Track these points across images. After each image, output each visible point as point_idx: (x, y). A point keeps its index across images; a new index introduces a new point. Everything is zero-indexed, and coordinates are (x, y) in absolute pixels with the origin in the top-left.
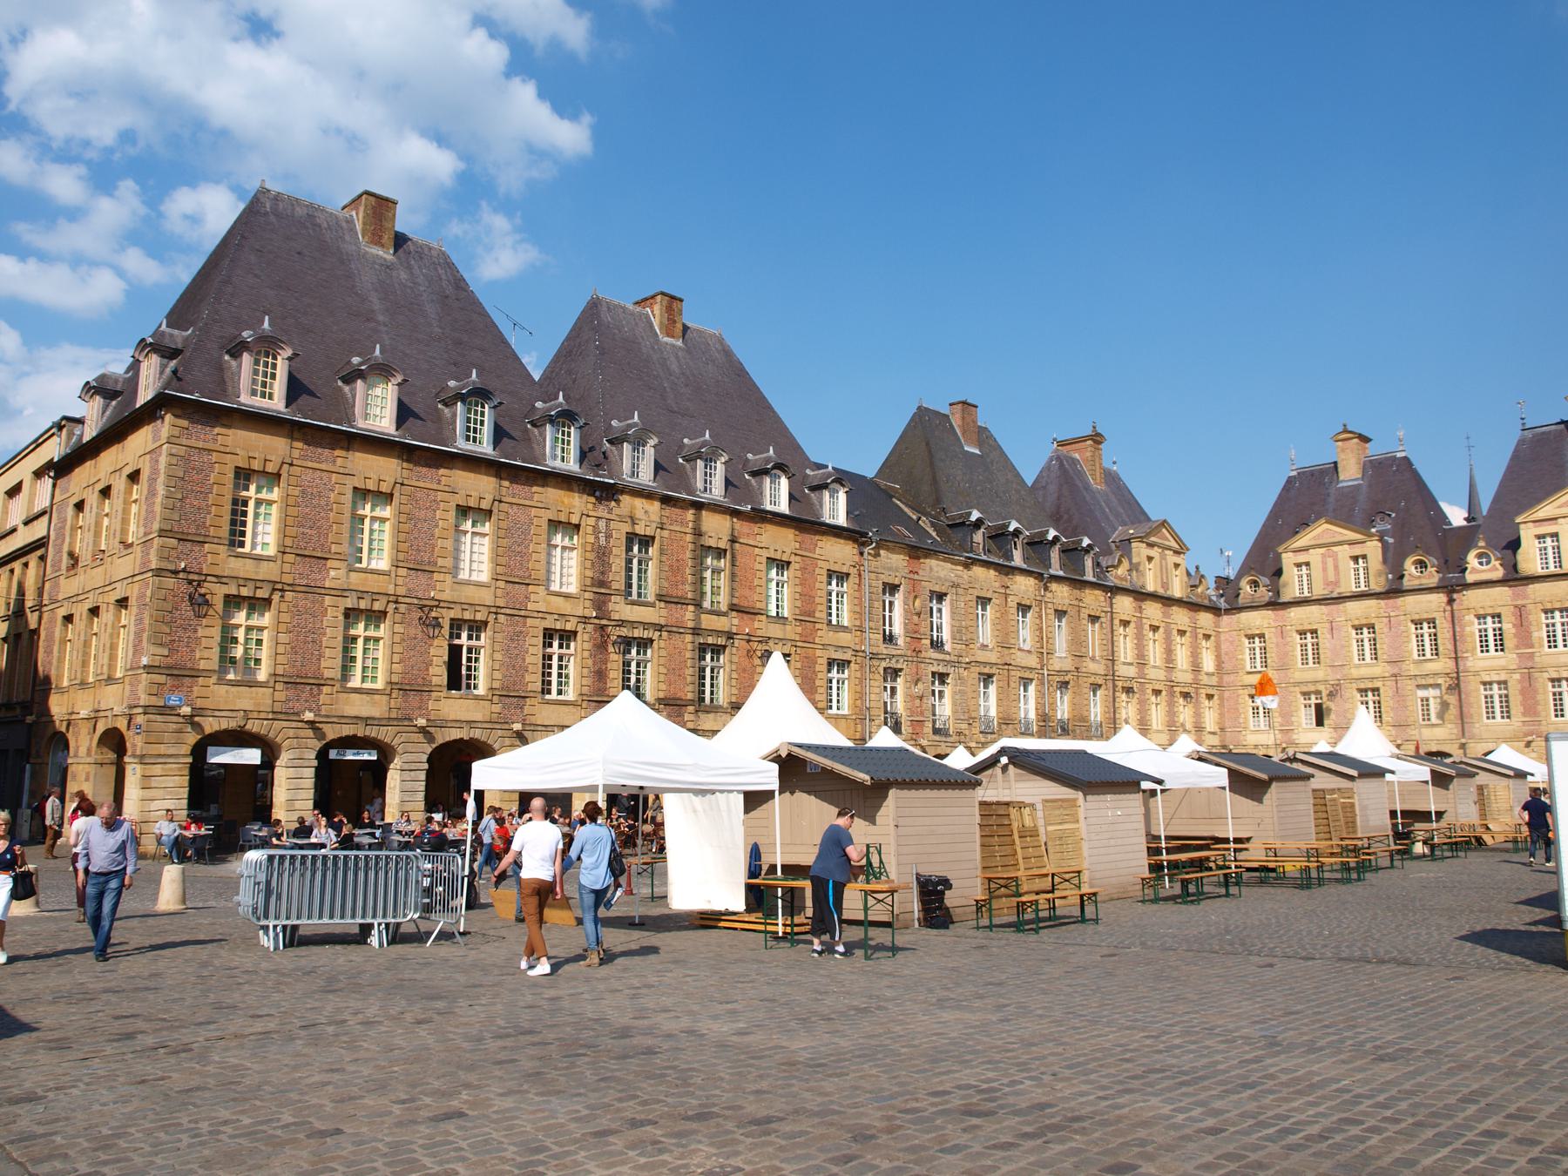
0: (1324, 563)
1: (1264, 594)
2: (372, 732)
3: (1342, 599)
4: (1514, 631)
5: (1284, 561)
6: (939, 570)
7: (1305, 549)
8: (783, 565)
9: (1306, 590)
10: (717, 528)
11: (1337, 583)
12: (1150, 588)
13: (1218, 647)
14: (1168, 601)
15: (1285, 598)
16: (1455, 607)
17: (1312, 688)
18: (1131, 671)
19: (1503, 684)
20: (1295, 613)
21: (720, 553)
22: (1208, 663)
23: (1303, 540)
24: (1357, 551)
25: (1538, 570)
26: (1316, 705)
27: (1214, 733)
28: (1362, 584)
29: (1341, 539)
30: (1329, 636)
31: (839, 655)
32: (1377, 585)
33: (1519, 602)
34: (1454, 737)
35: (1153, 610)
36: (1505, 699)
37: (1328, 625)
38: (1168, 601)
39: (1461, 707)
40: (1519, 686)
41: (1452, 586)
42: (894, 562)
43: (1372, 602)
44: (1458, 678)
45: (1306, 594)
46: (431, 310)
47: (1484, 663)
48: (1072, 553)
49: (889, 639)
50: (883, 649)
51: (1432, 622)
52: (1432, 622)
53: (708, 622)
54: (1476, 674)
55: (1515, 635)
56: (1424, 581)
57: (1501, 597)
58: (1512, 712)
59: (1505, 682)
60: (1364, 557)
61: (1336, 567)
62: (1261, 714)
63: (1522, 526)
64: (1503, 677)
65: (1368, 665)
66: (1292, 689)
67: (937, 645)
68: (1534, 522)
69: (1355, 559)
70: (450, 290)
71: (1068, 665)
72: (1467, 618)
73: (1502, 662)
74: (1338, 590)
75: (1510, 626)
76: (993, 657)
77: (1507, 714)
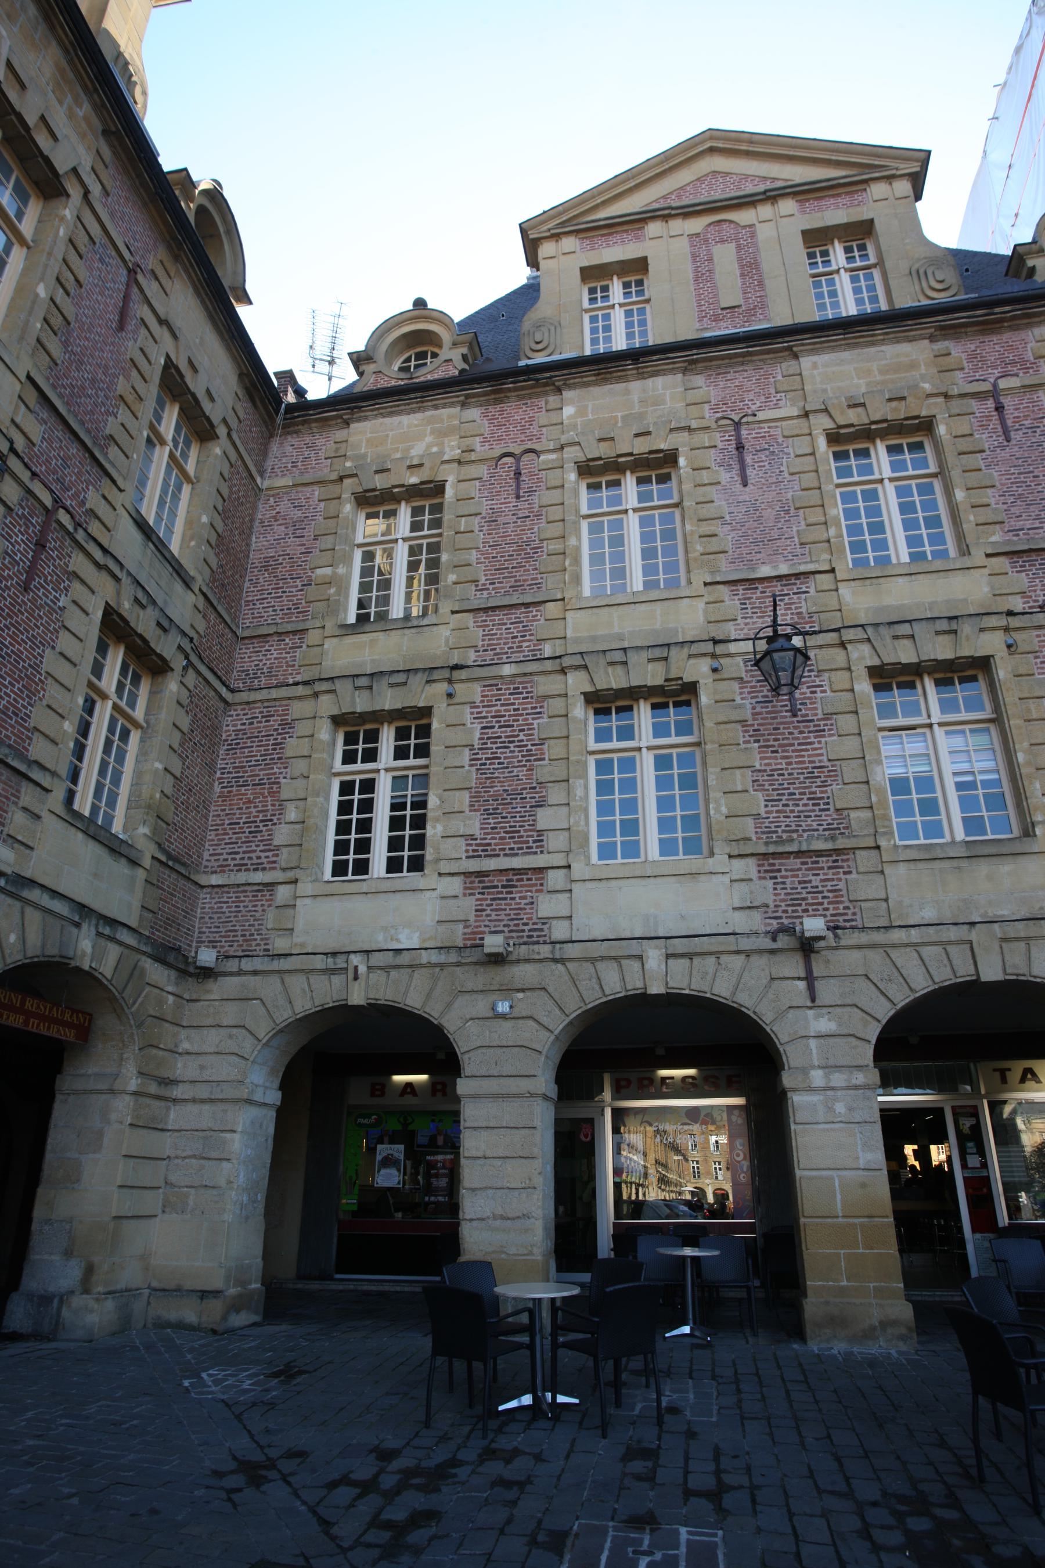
37: (722, 439)
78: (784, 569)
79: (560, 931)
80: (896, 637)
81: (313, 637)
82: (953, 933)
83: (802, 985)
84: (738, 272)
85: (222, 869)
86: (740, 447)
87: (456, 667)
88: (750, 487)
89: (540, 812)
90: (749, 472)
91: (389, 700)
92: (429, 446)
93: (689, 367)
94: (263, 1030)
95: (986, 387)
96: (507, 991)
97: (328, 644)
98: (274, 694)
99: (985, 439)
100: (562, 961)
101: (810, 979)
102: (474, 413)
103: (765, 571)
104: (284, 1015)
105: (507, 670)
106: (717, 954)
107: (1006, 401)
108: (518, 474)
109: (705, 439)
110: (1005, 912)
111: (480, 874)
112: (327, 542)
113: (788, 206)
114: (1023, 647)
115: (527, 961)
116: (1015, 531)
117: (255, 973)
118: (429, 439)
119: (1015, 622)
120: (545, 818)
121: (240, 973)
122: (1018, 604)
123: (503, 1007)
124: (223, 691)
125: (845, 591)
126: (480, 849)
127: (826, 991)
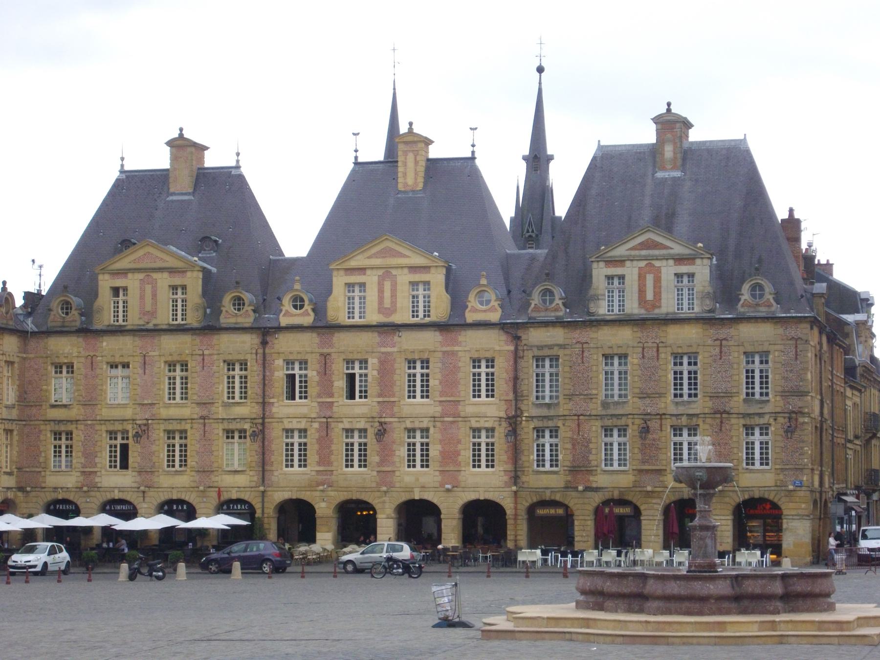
0: (142, 290)
1: (75, 319)
3: (157, 331)
4: (317, 379)
5: (100, 283)
7: (124, 273)
9: (121, 318)
11: (153, 314)
13: (21, 376)
15: (97, 326)
16: (267, 351)
17: (118, 427)
19: (303, 432)
20: (109, 346)
23: (125, 262)
24: (177, 281)
25: (344, 320)
26: (122, 445)
27: (10, 474)
28: (179, 317)
29: (159, 264)
30: (141, 371)
32: (193, 319)
33: (325, 351)
34: (254, 484)
36: (303, 447)
37: (140, 359)
39: (264, 454)
40: (317, 435)
43: (187, 338)
44: (263, 424)
45: (121, 322)
51: (244, 365)
52: (244, 365)
54: (280, 420)
55: (318, 384)
56: (240, 320)
58: (309, 461)
59: (305, 431)
60: (184, 287)
61: (154, 295)
62: (63, 454)
63: (335, 273)
64: (302, 426)
65: (177, 405)
66: (98, 427)
68: (347, 270)
69: (174, 288)
72: (277, 362)
73: (304, 410)
74: (154, 322)
75: (315, 373)
77: (303, 463)
78: (150, 402)
79: (99, 485)
80: (169, 423)
81: (44, 407)
82: (169, 490)
83: (142, 498)
84: (151, 297)
85: (29, 467)
86: (145, 363)
87: (78, 420)
88: (146, 376)
89: (96, 459)
90: (147, 371)
91: (63, 428)
92: (69, 350)
93: (134, 336)
94: (42, 503)
95: (201, 352)
96: (89, 497)
97: (48, 410)
98: (36, 423)
99: (198, 368)
100: (99, 491)
101: (144, 497)
102: (81, 340)
103: (146, 402)
104: (45, 500)
105: (89, 422)
106: (128, 492)
107: (206, 358)
108: (92, 363)
109: (137, 359)
110: (179, 486)
111: (84, 472)
112: (44, 378)
113: (166, 275)
114: (194, 427)
115: (93, 491)
116: (199, 396)
117: (39, 491)
118: (69, 347)
119: (193, 421)
120: (97, 460)
121: (35, 491)
122: (195, 416)
123: (88, 500)
124: (24, 423)
125: (162, 410)
126: (84, 466)
127: (147, 499)
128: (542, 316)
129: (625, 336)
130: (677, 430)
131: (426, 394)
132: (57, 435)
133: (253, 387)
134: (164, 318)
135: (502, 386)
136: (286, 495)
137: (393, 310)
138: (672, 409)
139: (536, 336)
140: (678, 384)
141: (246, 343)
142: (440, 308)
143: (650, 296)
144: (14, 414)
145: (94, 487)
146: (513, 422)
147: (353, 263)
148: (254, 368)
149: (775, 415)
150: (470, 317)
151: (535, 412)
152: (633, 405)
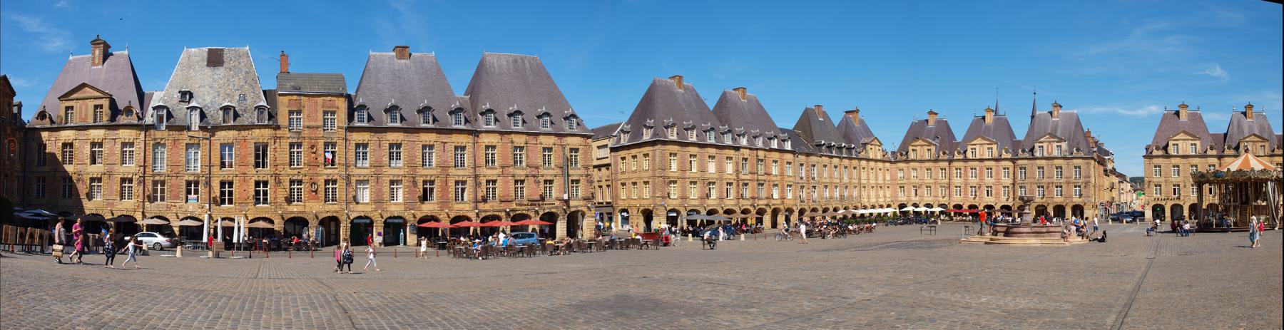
2: (696, 208)
6: (813, 159)
8: (776, 162)
10: (761, 154)
12: (871, 157)
14: (876, 161)
18: (866, 182)
19: (960, 187)
20: (912, 164)
21: (762, 160)
22: (888, 177)
31: (790, 184)
35: (872, 164)
38: (876, 161)
41: (950, 161)
42: (802, 158)
46: (694, 105)
47: (957, 181)
48: (849, 149)
49: (802, 178)
50: (800, 181)
52: (945, 169)
53: (760, 178)
57: (961, 164)
67: (813, 179)
70: (696, 98)
71: (847, 181)
76: (827, 181)
77: (960, 195)
128: (1022, 156)
129: (1043, 162)
130: (1057, 187)
131: (992, 177)
132: (901, 187)
133: (947, 175)
134: (927, 157)
135: (1011, 175)
136: (955, 203)
137: (983, 155)
138: (1055, 181)
139: (1020, 162)
140: (1057, 175)
141: (947, 164)
142: (996, 154)
143: (1050, 151)
144: (890, 182)
145: (910, 200)
146: (1014, 184)
147: (972, 143)
148: (947, 169)
149: (1082, 183)
150: (1003, 157)
151: (1020, 182)
152: (1046, 180)
